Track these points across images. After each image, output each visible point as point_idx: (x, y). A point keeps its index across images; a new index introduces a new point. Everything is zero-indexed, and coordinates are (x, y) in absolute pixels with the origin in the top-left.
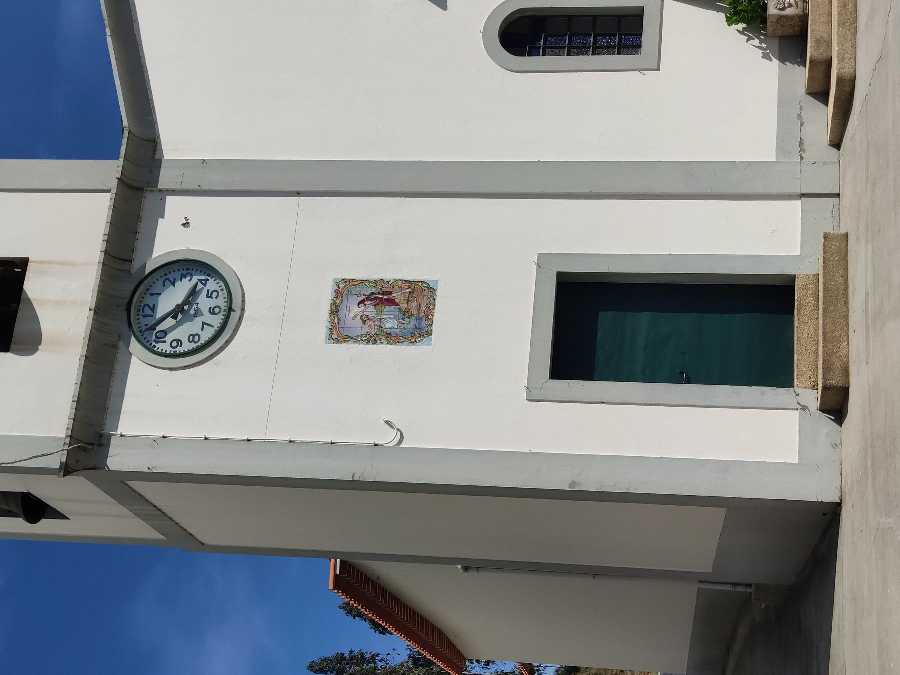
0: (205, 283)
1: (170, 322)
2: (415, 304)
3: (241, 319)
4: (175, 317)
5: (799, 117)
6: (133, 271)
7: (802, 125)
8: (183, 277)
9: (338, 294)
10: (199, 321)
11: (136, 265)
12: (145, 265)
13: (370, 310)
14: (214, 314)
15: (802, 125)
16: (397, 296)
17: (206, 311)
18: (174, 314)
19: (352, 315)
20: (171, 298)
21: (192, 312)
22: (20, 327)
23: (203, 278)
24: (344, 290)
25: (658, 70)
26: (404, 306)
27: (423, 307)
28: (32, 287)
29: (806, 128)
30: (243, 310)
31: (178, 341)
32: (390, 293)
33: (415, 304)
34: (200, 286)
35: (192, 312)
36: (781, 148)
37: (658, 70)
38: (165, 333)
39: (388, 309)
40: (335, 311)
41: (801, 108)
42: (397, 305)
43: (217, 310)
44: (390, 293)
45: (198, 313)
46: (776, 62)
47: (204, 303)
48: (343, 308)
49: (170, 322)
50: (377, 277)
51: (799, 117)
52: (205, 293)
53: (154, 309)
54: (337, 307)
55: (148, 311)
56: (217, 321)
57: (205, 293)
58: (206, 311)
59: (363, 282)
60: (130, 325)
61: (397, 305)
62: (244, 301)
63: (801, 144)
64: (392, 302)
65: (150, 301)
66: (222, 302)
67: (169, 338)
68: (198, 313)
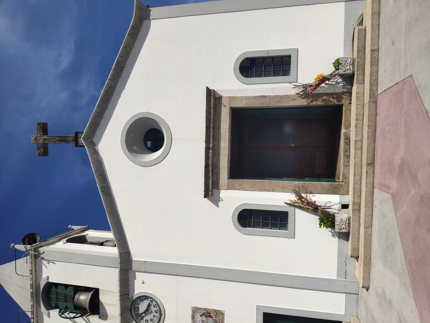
0: (152, 301)
1: (144, 315)
2: (218, 318)
3: (165, 317)
4: (145, 313)
5: (345, 262)
6: (130, 297)
7: (346, 265)
8: (145, 299)
9: (193, 312)
10: (152, 314)
11: (130, 296)
12: (133, 297)
13: (204, 319)
14: (156, 313)
15: (346, 265)
16: (212, 314)
17: (154, 312)
18: (144, 313)
19: (198, 319)
20: (143, 307)
21: (150, 311)
22: (101, 311)
23: (151, 300)
24: (195, 310)
25: (294, 238)
26: (214, 318)
27: (221, 319)
28: (102, 298)
29: (348, 266)
30: (165, 314)
31: (147, 320)
32: (210, 313)
33: (218, 318)
34: (151, 303)
35: (150, 311)
36: (338, 274)
37: (294, 238)
38: (143, 317)
39: (210, 319)
40: (193, 318)
41: (346, 258)
42: (212, 317)
43: (157, 312)
44: (210, 313)
45: (151, 312)
46: (337, 238)
47: (153, 309)
48: (195, 317)
49: (144, 315)
50: (205, 307)
51: (345, 262)
52: (152, 306)
53: (138, 309)
54: (194, 316)
55: (137, 309)
56: (158, 315)
57: (152, 306)
58: (154, 312)
59: (201, 309)
60: (132, 316)
61: (212, 317)
62: (165, 311)
63: (346, 273)
64: (210, 316)
65: (137, 306)
66: (157, 309)
67: (145, 319)
68: (151, 312)
